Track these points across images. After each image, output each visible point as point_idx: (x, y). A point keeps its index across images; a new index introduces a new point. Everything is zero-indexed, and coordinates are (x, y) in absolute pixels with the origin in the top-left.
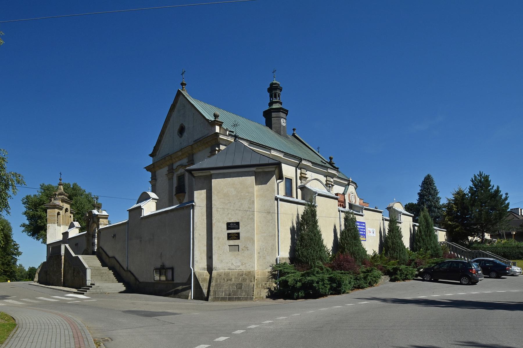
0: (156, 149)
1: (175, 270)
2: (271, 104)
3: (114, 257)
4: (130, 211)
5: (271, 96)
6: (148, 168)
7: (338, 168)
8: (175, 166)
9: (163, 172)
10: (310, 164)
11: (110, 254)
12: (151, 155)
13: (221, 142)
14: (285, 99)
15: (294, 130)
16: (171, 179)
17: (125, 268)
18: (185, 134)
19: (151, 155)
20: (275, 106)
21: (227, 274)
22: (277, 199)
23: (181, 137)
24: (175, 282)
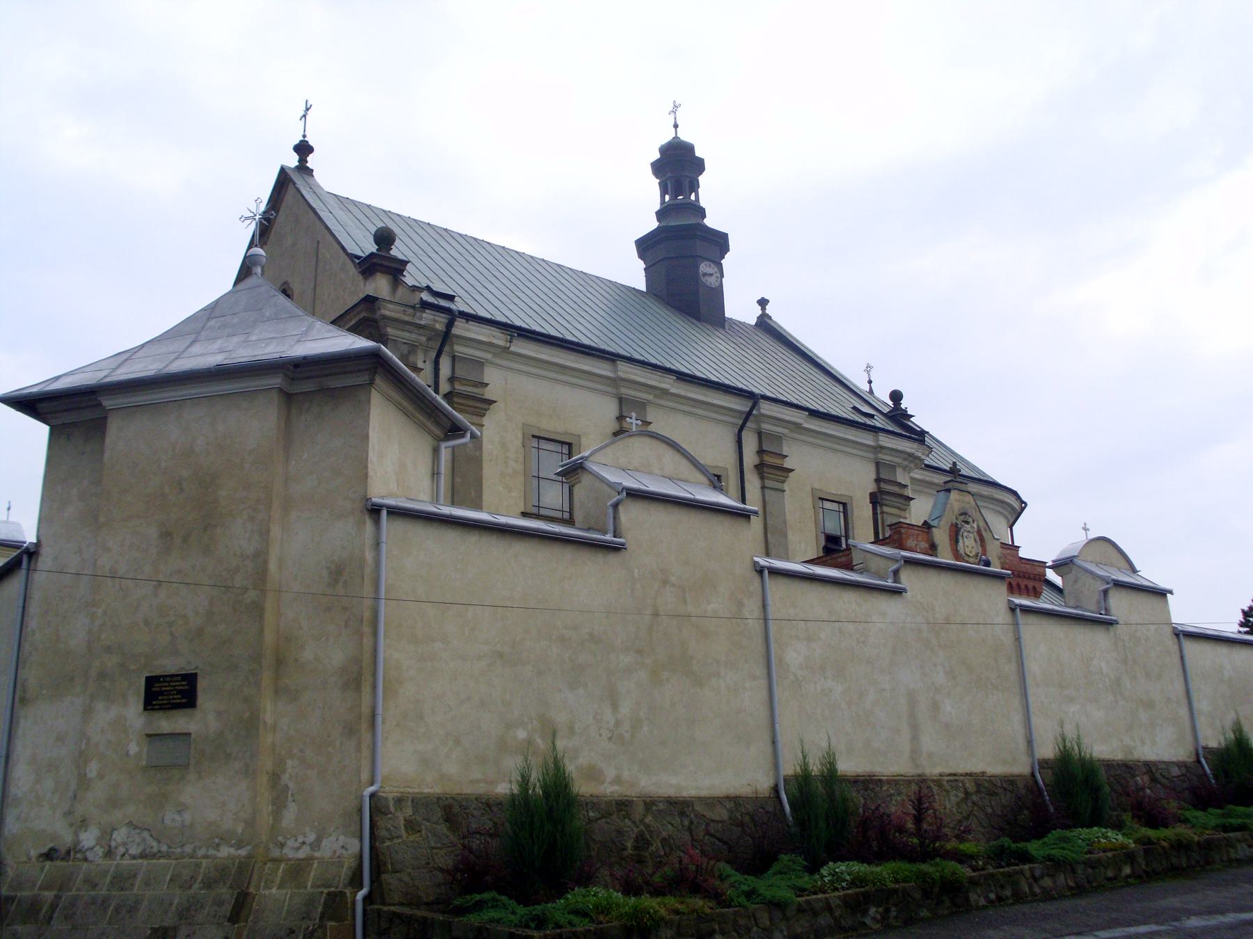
15: (763, 303)
21: (122, 880)
22: (375, 511)
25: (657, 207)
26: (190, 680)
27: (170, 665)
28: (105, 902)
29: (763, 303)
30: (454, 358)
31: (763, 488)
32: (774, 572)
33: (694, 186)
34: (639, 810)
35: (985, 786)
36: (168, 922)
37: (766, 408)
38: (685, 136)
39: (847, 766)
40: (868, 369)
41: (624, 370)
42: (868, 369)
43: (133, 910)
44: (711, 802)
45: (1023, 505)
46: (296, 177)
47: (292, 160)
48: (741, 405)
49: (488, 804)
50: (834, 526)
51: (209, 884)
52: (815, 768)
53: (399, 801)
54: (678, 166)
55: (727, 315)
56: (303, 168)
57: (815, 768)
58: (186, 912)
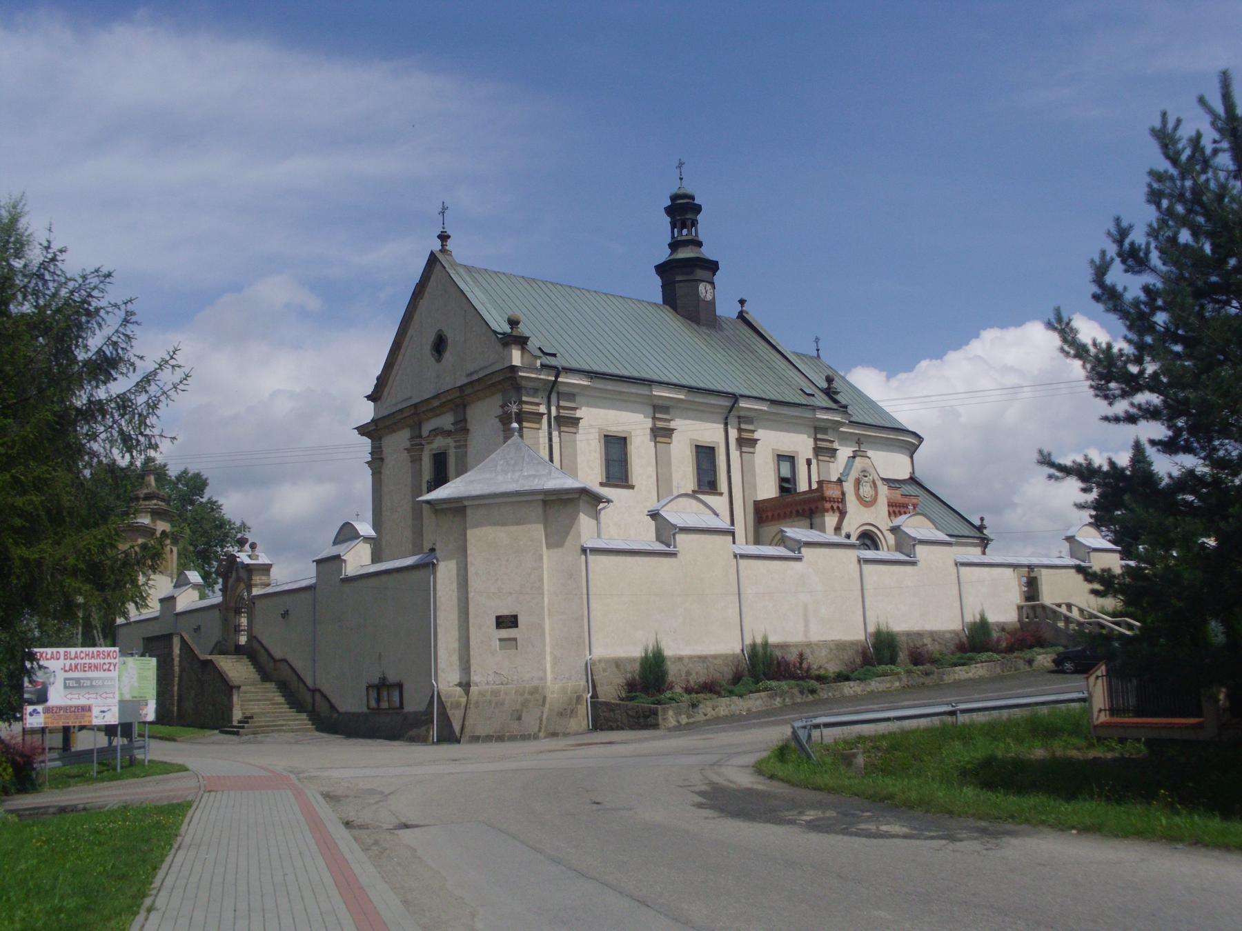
0: (382, 381)
1: (405, 688)
2: (674, 246)
3: (286, 661)
4: (318, 562)
5: (673, 225)
6: (363, 430)
7: (845, 407)
8: (426, 430)
9: (398, 442)
10: (764, 407)
11: (278, 654)
12: (369, 398)
13: (524, 383)
14: (713, 234)
15: (742, 302)
16: (416, 460)
17: (310, 683)
18: (448, 355)
19: (369, 398)
20: (683, 254)
21: (495, 693)
22: (584, 550)
23: (439, 360)
24: (406, 710)
25: (669, 240)
26: (515, 617)
27: (505, 612)
28: (490, 702)
29: (742, 302)
30: (558, 393)
31: (741, 453)
32: (743, 556)
33: (694, 223)
34: (686, 661)
35: (841, 646)
36: (519, 707)
37: (743, 404)
38: (688, 189)
39: (773, 639)
40: (817, 340)
41: (658, 392)
42: (817, 340)
43: (502, 704)
44: (715, 657)
45: (920, 439)
46: (440, 256)
47: (436, 245)
48: (727, 403)
49: (632, 660)
50: (786, 471)
51: (531, 693)
52: (759, 641)
53: (600, 661)
54: (683, 211)
55: (718, 313)
56: (443, 250)
57: (759, 641)
58: (525, 704)
